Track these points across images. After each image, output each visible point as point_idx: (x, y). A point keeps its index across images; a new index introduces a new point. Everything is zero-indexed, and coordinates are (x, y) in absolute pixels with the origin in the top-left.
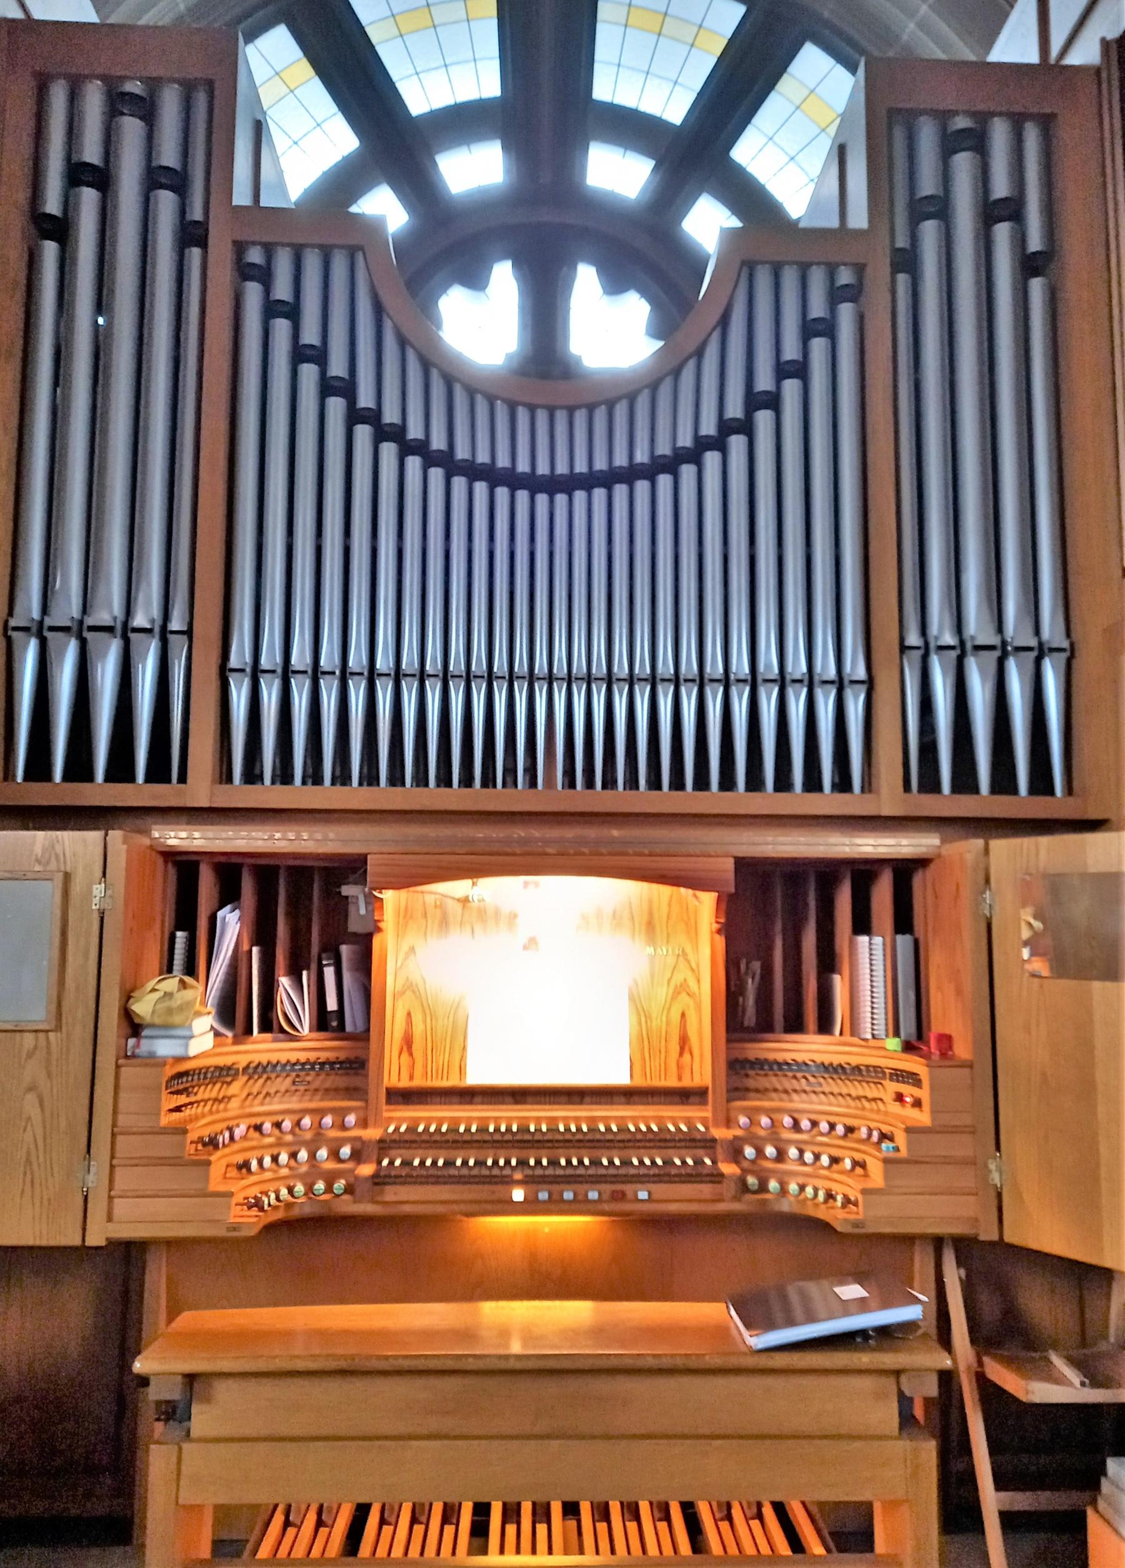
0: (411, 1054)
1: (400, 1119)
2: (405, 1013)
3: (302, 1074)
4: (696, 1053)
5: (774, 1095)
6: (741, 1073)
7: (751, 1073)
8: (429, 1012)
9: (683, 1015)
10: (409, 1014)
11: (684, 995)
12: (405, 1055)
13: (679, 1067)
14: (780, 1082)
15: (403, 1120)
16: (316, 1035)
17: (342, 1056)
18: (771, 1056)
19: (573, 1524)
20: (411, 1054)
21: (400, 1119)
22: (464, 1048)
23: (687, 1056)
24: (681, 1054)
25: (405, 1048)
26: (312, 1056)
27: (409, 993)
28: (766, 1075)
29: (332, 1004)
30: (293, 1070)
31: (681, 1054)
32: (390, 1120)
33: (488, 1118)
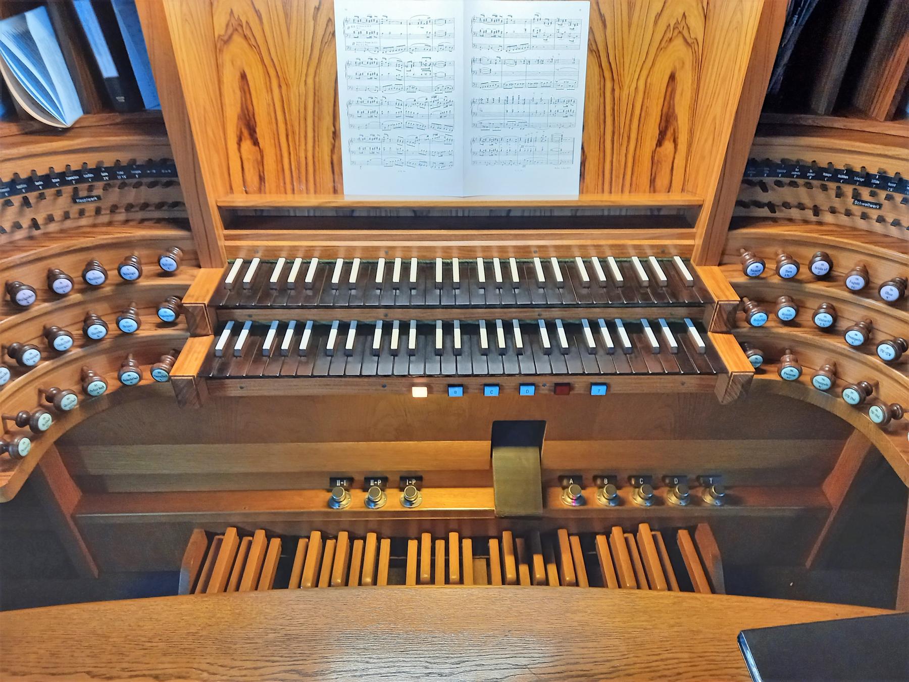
0: (256, 143)
1: (243, 257)
2: (238, 75)
3: (83, 186)
4: (683, 138)
5: (795, 213)
6: (757, 186)
7: (769, 181)
8: (277, 77)
9: (672, 77)
10: (243, 76)
11: (678, 42)
12: (247, 144)
13: (654, 162)
14: (812, 197)
15: (253, 251)
16: (93, 119)
17: (141, 157)
18: (808, 157)
19: (482, 563)
20: (256, 143)
21: (243, 257)
22: (336, 135)
23: (668, 145)
24: (660, 143)
25: (246, 133)
26: (92, 160)
27: (237, 39)
28: (793, 184)
29: (108, 69)
30: (64, 182)
31: (660, 143)
32: (233, 252)
33: (377, 248)
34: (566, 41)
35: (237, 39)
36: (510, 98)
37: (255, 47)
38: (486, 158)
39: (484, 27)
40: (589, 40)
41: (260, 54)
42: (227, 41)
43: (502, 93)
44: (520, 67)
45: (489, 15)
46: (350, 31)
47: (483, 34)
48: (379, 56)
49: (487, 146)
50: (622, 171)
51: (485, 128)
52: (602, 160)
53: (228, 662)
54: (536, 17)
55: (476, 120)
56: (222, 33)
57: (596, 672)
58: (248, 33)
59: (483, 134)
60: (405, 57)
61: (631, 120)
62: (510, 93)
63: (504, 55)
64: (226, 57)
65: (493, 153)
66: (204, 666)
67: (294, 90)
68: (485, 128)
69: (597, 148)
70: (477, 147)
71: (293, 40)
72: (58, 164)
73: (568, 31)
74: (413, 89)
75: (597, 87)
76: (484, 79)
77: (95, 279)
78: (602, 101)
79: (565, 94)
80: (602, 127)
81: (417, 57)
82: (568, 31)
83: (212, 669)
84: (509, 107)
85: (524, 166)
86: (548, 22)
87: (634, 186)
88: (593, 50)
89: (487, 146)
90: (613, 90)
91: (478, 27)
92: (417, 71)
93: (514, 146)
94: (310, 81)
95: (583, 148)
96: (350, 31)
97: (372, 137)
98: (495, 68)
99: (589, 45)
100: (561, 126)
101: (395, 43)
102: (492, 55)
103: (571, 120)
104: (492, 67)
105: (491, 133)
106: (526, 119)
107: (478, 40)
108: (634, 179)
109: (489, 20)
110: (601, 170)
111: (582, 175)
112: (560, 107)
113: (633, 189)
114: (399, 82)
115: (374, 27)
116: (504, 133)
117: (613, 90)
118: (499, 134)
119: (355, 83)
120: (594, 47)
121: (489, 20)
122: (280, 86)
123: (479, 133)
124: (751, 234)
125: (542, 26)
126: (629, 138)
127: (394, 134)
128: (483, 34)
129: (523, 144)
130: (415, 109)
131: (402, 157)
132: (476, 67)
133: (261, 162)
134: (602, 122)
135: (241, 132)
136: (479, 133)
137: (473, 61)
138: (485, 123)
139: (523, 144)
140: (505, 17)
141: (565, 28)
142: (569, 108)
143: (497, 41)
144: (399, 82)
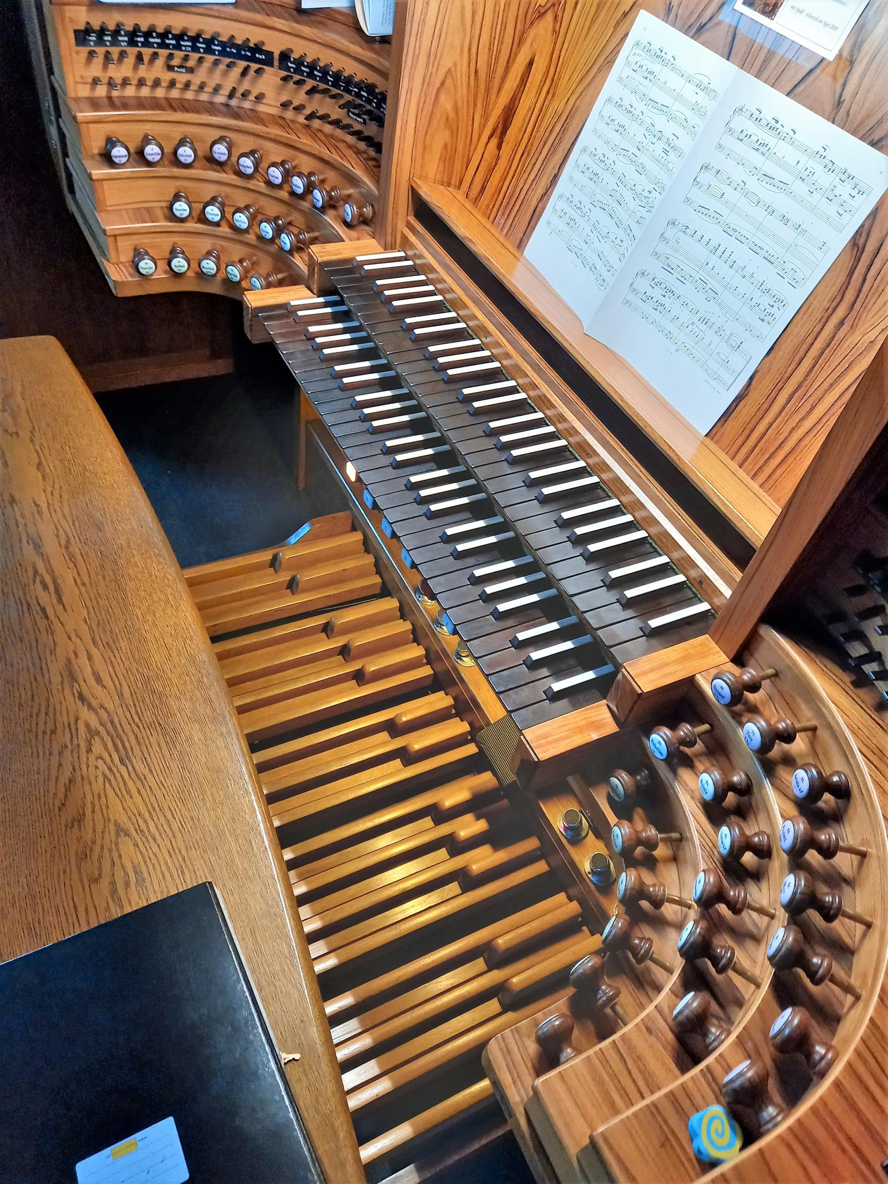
0: (499, 147)
10: (531, 63)
12: (494, 142)
20: (499, 147)
22: (556, 178)
34: (831, 209)
35: (549, 17)
36: (721, 249)
37: (556, 33)
38: (648, 308)
39: (751, 127)
40: (862, 226)
41: (555, 44)
42: (541, 15)
43: (713, 232)
44: (759, 213)
45: (767, 116)
46: (633, 59)
47: (743, 137)
48: (640, 106)
49: (657, 293)
50: (772, 449)
51: (668, 269)
52: (761, 413)
53: (65, 497)
54: (822, 152)
55: (662, 249)
56: (543, 4)
57: (134, 761)
58: (560, 14)
59: (662, 275)
60: (661, 122)
61: (831, 385)
62: (729, 243)
63: (753, 184)
64: (532, 33)
65: (659, 306)
66: (57, 486)
67: (555, 103)
68: (668, 269)
69: (767, 392)
70: (643, 285)
71: (586, 43)
72: (350, 68)
73: (845, 196)
74: (641, 170)
75: (826, 304)
76: (713, 205)
77: (296, 186)
78: (817, 329)
79: (781, 287)
80: (793, 366)
81: (669, 129)
82: (845, 196)
83: (57, 493)
84: (714, 260)
85: (677, 350)
86: (831, 167)
87: (771, 482)
88: (857, 245)
89: (657, 293)
90: (842, 323)
91: (741, 123)
92: (660, 146)
93: (685, 316)
94: (571, 102)
95: (751, 378)
96: (633, 59)
97: (578, 205)
98: (732, 195)
99: (858, 233)
100: (749, 329)
101: (663, 98)
102: (738, 174)
103: (764, 328)
104: (728, 190)
105: (671, 281)
106: (719, 289)
107: (730, 142)
108: (779, 472)
109: (764, 122)
110: (751, 426)
111: (727, 415)
112: (765, 301)
113: (767, 486)
114: (636, 152)
115: (656, 67)
116: (686, 291)
117: (842, 323)
118: (678, 287)
119: (602, 127)
120: (862, 241)
121: (764, 122)
122: (548, 92)
123: (655, 268)
124: (788, 655)
125: (819, 169)
126: (812, 409)
127: (597, 214)
128: (743, 137)
129: (696, 321)
130: (628, 195)
131: (584, 246)
132: (705, 178)
133: (491, 170)
134: (797, 359)
135: (497, 126)
136: (655, 268)
137: (705, 167)
138: (674, 262)
139: (696, 321)
140: (787, 129)
141: (844, 190)
142: (772, 311)
143: (756, 158)
144: (636, 152)
